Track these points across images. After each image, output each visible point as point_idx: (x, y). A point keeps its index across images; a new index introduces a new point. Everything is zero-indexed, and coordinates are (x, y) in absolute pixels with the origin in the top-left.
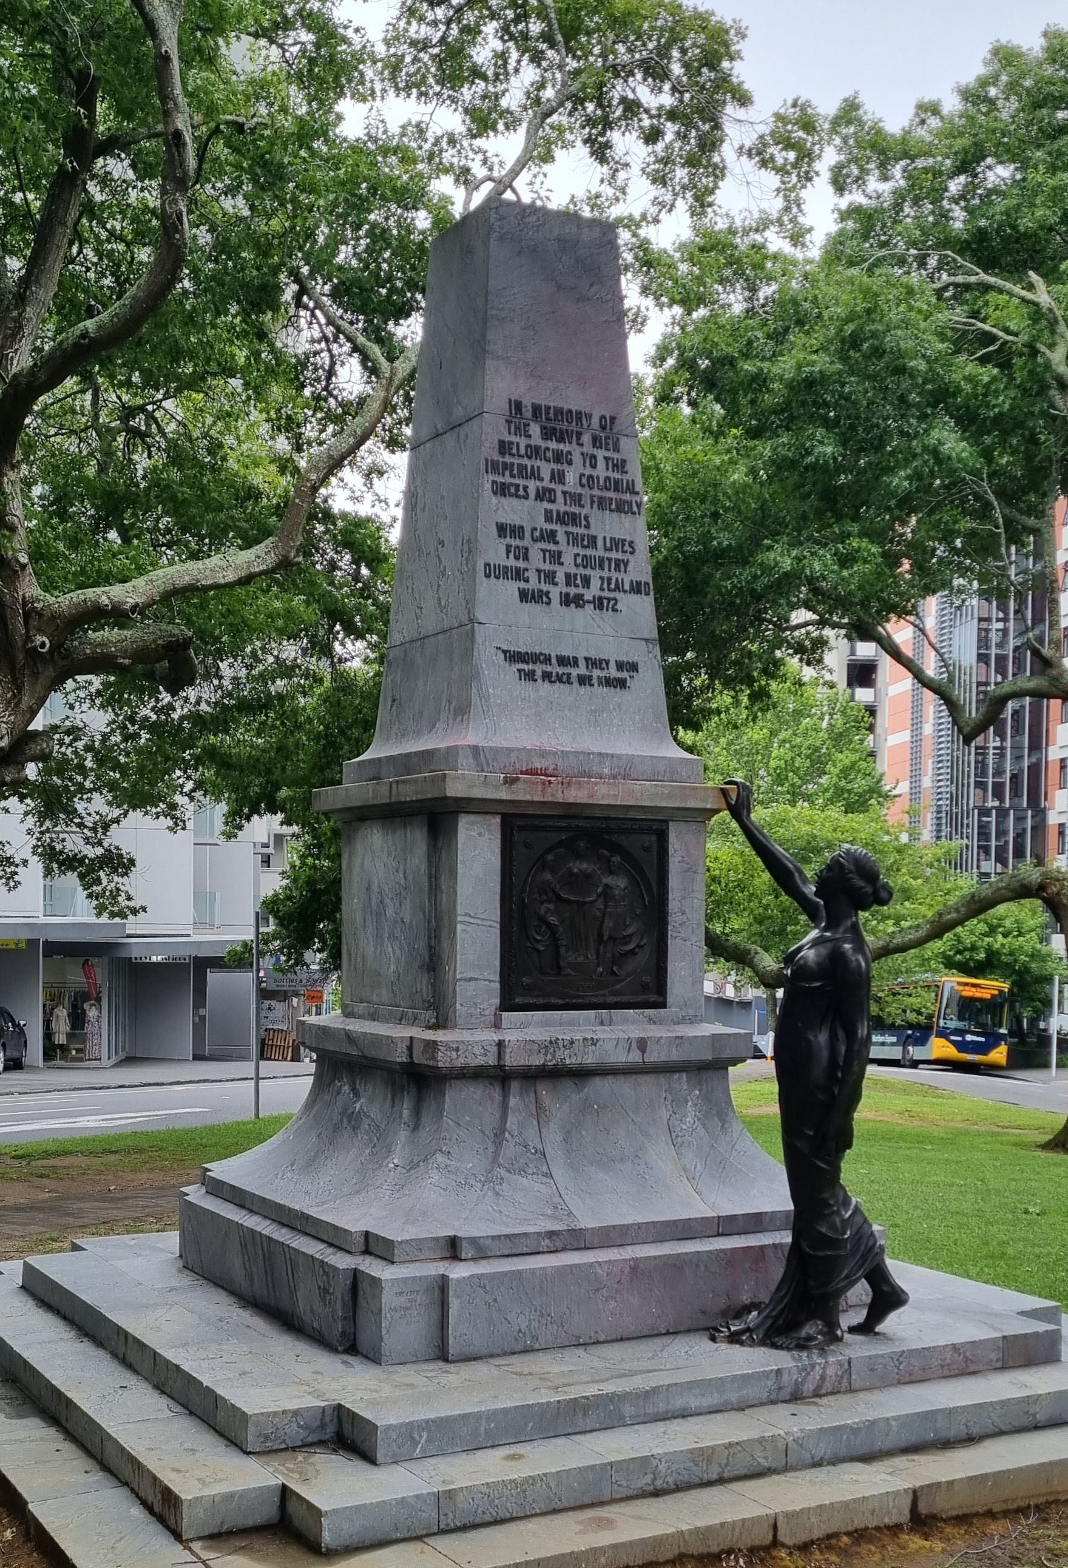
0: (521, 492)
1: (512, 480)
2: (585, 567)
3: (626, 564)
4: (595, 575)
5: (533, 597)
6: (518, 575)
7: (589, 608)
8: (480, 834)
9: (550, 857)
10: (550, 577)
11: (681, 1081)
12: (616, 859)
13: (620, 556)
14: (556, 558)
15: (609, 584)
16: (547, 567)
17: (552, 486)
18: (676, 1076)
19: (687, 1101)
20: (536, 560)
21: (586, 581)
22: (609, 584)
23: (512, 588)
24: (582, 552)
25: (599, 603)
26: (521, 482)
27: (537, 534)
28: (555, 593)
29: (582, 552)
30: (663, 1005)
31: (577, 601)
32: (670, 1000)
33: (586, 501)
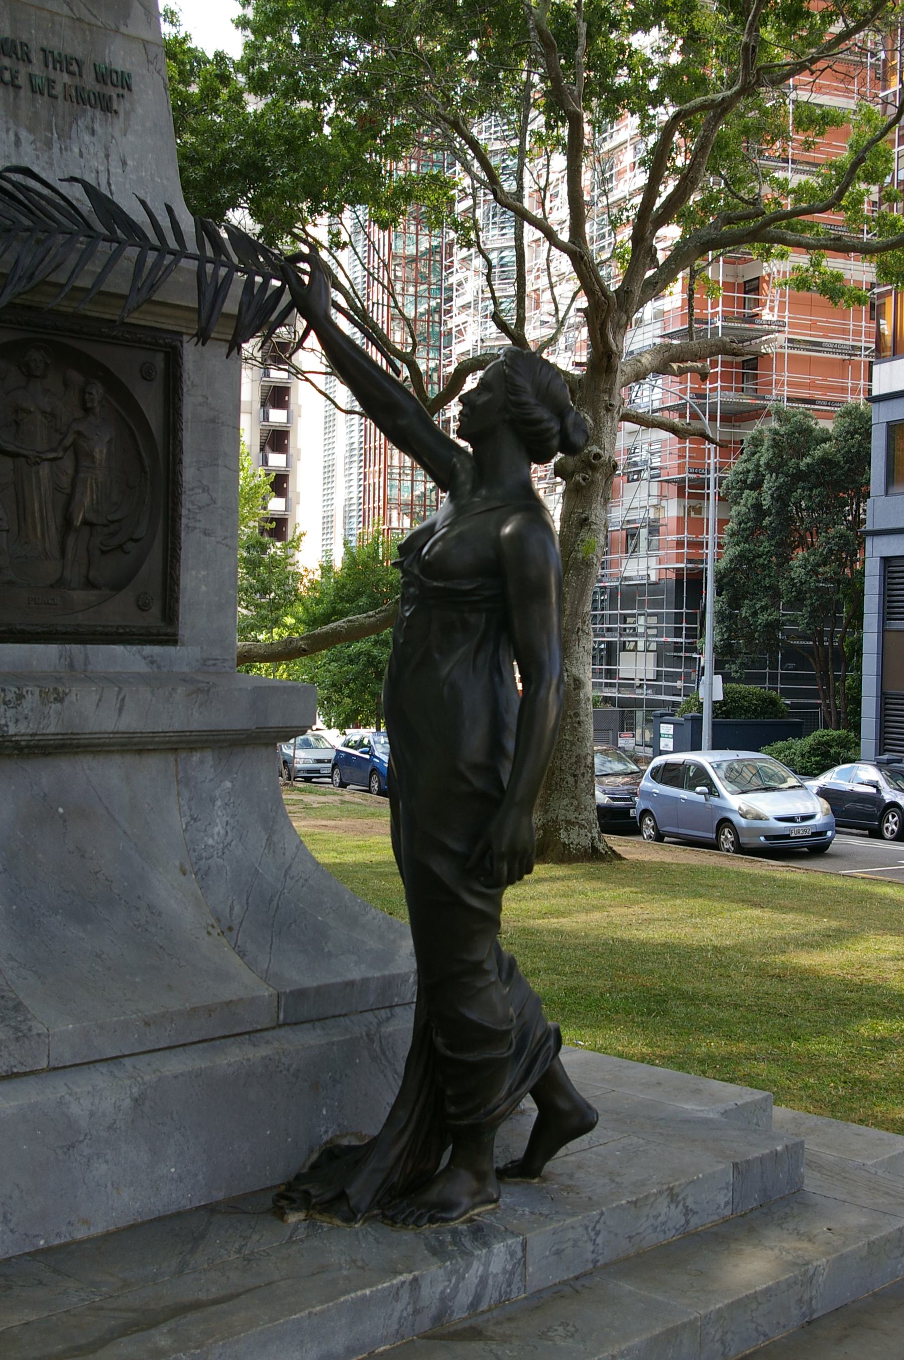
11: (204, 766)
12: (97, 391)
18: (196, 757)
19: (213, 800)
30: (171, 639)
32: (184, 631)
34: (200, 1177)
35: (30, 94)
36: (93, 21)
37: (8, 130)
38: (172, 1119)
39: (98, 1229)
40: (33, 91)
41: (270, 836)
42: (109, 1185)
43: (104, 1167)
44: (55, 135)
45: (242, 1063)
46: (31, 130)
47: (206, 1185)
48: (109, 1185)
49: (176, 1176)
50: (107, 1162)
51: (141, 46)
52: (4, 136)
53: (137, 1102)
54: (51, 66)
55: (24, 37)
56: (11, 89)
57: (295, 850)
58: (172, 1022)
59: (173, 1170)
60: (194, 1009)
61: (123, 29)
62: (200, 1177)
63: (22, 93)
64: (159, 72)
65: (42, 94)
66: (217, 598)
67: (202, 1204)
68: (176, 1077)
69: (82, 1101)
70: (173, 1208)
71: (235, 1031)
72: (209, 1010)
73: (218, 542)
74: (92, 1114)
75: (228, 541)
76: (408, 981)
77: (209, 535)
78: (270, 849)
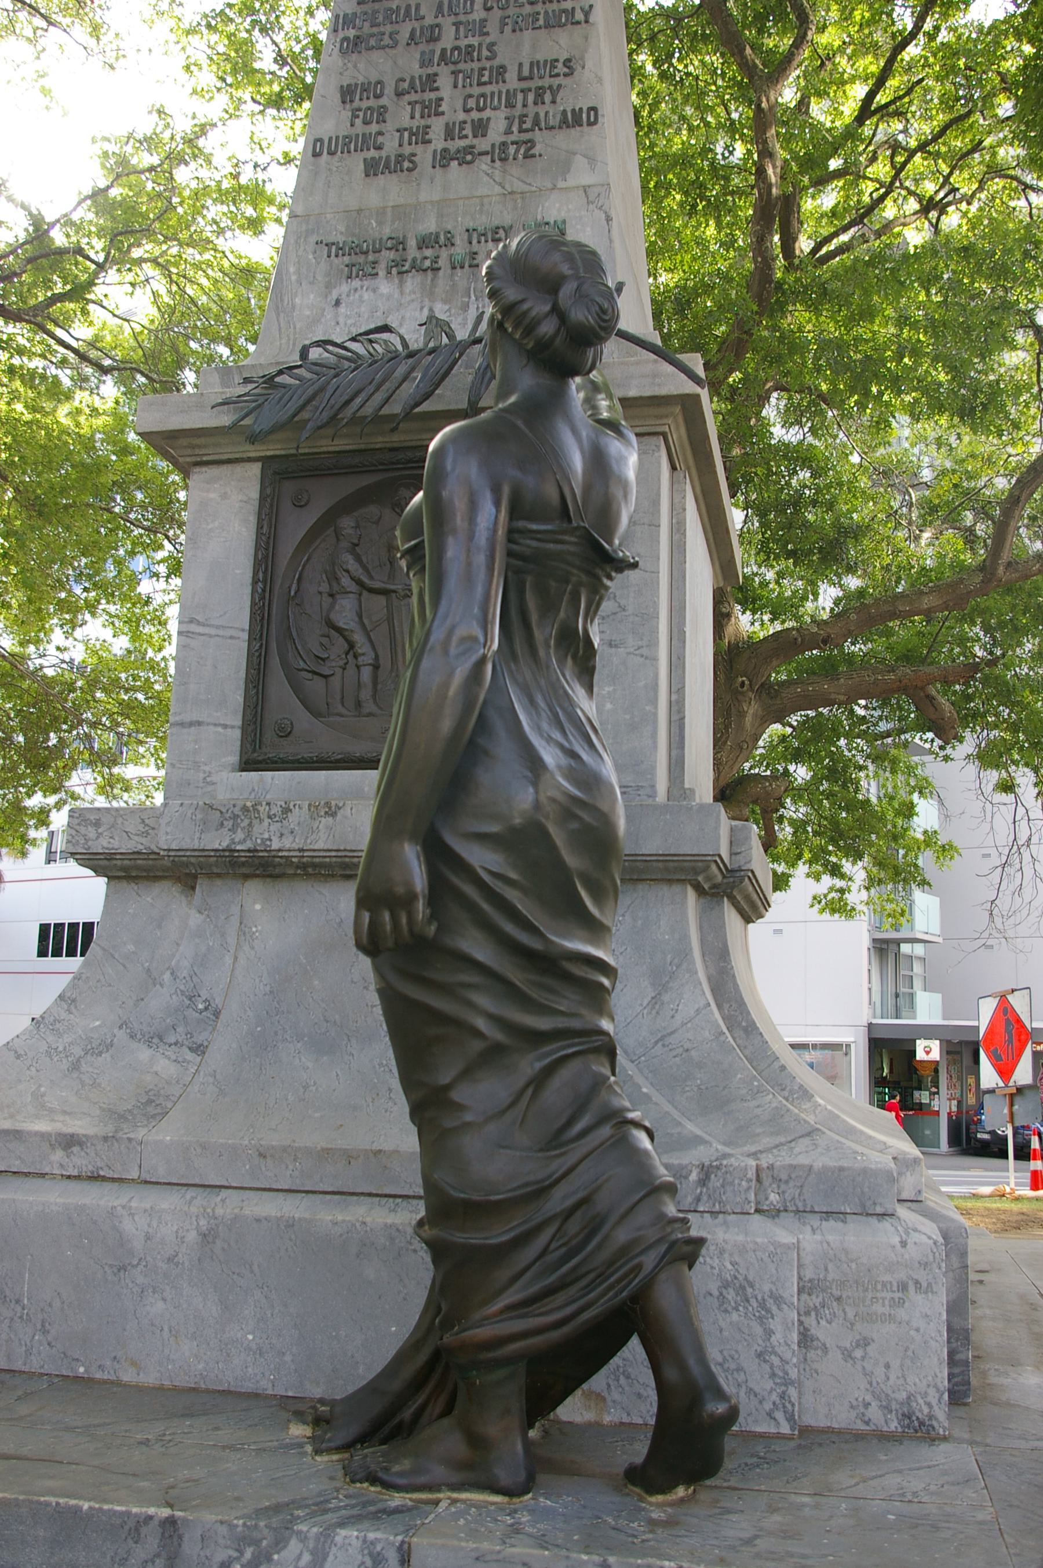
0: (387, 40)
1: (375, 30)
2: (480, 110)
3: (555, 91)
4: (498, 122)
5: (387, 166)
6: (366, 142)
7: (484, 164)
8: (224, 496)
9: (347, 523)
10: (421, 136)
13: (546, 82)
14: (433, 109)
15: (522, 122)
16: (418, 122)
17: (440, 20)
20: (401, 115)
21: (481, 128)
22: (522, 122)
23: (357, 162)
24: (476, 91)
25: (500, 154)
26: (388, 29)
27: (406, 85)
28: (424, 155)
29: (476, 91)
31: (466, 157)
33: (492, 27)
34: (288, 1358)
35: (449, 271)
36: (526, 188)
37: (422, 308)
38: (252, 1272)
39: (150, 1378)
40: (454, 268)
41: (659, 994)
42: (166, 1329)
43: (160, 1305)
44: (473, 298)
45: (354, 1225)
46: (445, 301)
47: (296, 1371)
48: (166, 1329)
49: (254, 1347)
50: (164, 1300)
51: (581, 192)
52: (417, 314)
53: (207, 1237)
54: (475, 241)
55: (449, 227)
56: (429, 272)
57: (692, 1013)
58: (295, 1160)
59: (250, 1337)
60: (327, 1151)
61: (561, 184)
62: (288, 1358)
63: (441, 273)
64: (600, 208)
65: (462, 267)
66: (628, 717)
67: (290, 1394)
68: (258, 1220)
69: (136, 1218)
70: (249, 1387)
71: (387, 1191)
72: (349, 1156)
73: (629, 653)
74: (148, 1238)
75: (644, 651)
76: (686, 1177)
77: (616, 646)
78: (653, 1008)
